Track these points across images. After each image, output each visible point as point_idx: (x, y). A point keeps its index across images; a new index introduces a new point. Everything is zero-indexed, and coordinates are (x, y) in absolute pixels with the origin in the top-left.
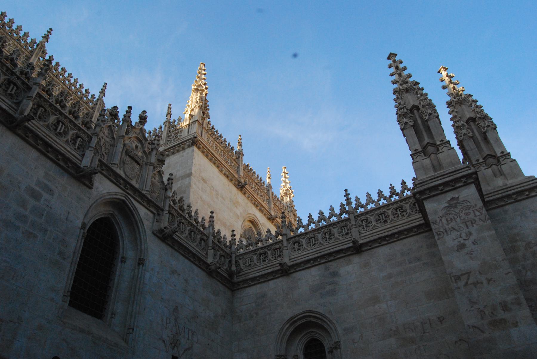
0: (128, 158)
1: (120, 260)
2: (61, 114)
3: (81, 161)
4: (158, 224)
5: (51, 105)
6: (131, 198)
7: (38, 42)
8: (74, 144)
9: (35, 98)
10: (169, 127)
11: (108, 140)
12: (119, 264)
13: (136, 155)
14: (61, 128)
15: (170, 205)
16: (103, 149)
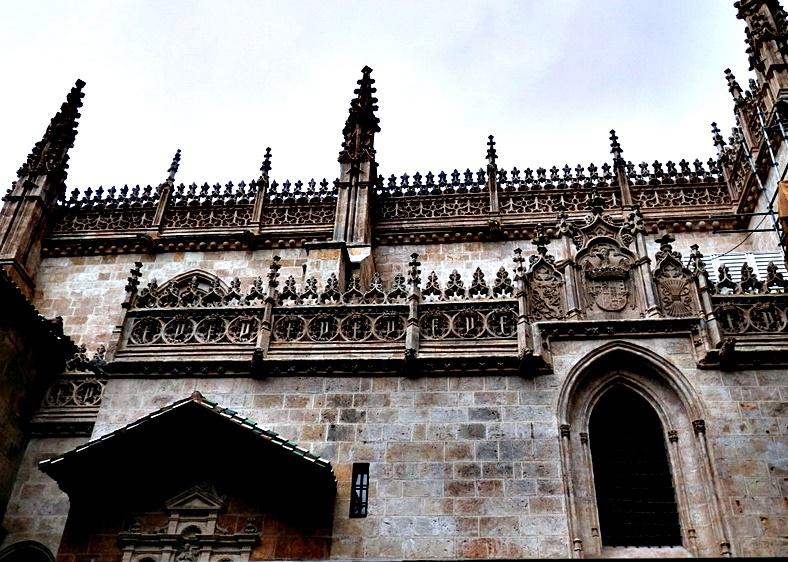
0: (594, 284)
1: (668, 440)
2: (460, 306)
3: (516, 346)
4: (699, 349)
5: (442, 307)
6: (627, 341)
7: (485, 170)
8: (499, 330)
9: (419, 316)
10: (745, 112)
11: (549, 283)
12: (669, 445)
13: (607, 269)
14: (469, 324)
15: (714, 301)
16: (547, 300)
